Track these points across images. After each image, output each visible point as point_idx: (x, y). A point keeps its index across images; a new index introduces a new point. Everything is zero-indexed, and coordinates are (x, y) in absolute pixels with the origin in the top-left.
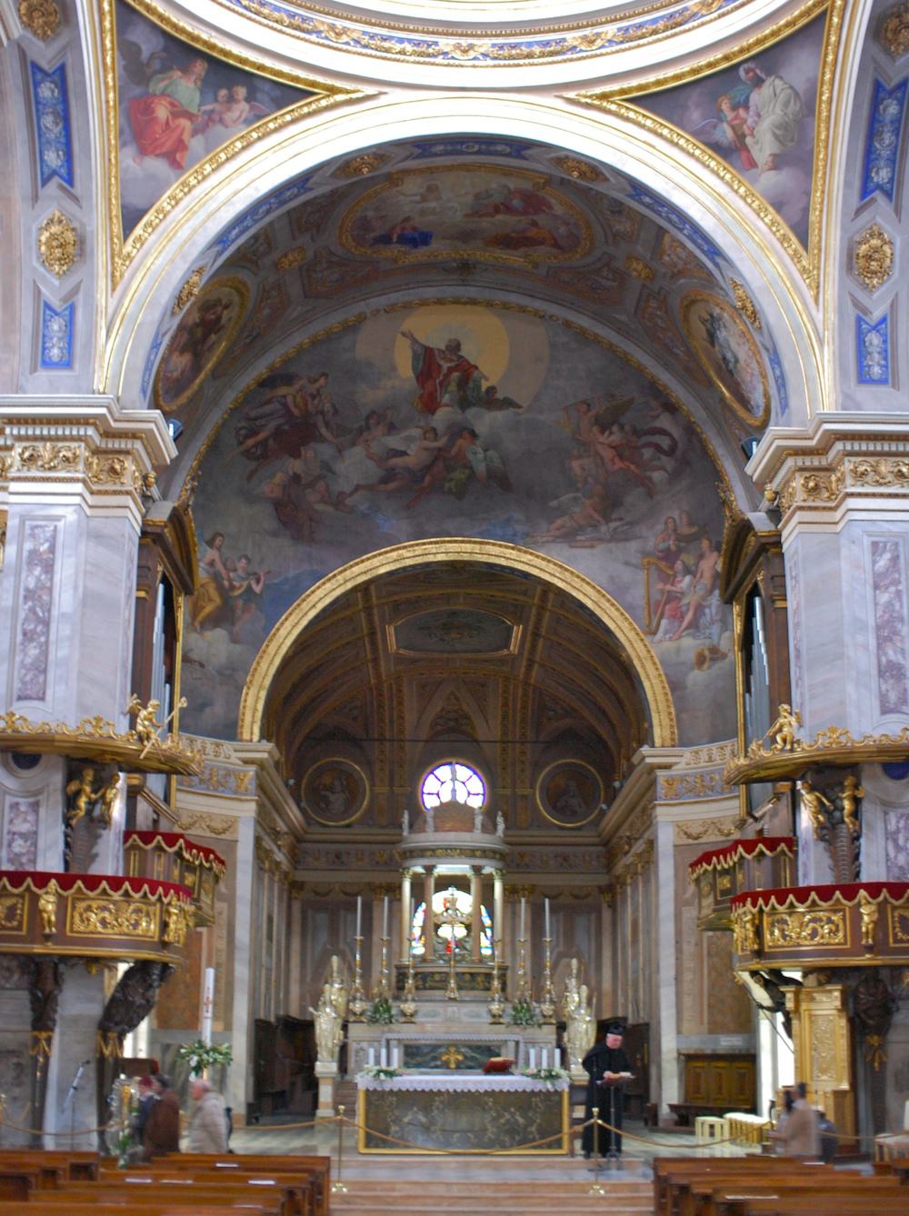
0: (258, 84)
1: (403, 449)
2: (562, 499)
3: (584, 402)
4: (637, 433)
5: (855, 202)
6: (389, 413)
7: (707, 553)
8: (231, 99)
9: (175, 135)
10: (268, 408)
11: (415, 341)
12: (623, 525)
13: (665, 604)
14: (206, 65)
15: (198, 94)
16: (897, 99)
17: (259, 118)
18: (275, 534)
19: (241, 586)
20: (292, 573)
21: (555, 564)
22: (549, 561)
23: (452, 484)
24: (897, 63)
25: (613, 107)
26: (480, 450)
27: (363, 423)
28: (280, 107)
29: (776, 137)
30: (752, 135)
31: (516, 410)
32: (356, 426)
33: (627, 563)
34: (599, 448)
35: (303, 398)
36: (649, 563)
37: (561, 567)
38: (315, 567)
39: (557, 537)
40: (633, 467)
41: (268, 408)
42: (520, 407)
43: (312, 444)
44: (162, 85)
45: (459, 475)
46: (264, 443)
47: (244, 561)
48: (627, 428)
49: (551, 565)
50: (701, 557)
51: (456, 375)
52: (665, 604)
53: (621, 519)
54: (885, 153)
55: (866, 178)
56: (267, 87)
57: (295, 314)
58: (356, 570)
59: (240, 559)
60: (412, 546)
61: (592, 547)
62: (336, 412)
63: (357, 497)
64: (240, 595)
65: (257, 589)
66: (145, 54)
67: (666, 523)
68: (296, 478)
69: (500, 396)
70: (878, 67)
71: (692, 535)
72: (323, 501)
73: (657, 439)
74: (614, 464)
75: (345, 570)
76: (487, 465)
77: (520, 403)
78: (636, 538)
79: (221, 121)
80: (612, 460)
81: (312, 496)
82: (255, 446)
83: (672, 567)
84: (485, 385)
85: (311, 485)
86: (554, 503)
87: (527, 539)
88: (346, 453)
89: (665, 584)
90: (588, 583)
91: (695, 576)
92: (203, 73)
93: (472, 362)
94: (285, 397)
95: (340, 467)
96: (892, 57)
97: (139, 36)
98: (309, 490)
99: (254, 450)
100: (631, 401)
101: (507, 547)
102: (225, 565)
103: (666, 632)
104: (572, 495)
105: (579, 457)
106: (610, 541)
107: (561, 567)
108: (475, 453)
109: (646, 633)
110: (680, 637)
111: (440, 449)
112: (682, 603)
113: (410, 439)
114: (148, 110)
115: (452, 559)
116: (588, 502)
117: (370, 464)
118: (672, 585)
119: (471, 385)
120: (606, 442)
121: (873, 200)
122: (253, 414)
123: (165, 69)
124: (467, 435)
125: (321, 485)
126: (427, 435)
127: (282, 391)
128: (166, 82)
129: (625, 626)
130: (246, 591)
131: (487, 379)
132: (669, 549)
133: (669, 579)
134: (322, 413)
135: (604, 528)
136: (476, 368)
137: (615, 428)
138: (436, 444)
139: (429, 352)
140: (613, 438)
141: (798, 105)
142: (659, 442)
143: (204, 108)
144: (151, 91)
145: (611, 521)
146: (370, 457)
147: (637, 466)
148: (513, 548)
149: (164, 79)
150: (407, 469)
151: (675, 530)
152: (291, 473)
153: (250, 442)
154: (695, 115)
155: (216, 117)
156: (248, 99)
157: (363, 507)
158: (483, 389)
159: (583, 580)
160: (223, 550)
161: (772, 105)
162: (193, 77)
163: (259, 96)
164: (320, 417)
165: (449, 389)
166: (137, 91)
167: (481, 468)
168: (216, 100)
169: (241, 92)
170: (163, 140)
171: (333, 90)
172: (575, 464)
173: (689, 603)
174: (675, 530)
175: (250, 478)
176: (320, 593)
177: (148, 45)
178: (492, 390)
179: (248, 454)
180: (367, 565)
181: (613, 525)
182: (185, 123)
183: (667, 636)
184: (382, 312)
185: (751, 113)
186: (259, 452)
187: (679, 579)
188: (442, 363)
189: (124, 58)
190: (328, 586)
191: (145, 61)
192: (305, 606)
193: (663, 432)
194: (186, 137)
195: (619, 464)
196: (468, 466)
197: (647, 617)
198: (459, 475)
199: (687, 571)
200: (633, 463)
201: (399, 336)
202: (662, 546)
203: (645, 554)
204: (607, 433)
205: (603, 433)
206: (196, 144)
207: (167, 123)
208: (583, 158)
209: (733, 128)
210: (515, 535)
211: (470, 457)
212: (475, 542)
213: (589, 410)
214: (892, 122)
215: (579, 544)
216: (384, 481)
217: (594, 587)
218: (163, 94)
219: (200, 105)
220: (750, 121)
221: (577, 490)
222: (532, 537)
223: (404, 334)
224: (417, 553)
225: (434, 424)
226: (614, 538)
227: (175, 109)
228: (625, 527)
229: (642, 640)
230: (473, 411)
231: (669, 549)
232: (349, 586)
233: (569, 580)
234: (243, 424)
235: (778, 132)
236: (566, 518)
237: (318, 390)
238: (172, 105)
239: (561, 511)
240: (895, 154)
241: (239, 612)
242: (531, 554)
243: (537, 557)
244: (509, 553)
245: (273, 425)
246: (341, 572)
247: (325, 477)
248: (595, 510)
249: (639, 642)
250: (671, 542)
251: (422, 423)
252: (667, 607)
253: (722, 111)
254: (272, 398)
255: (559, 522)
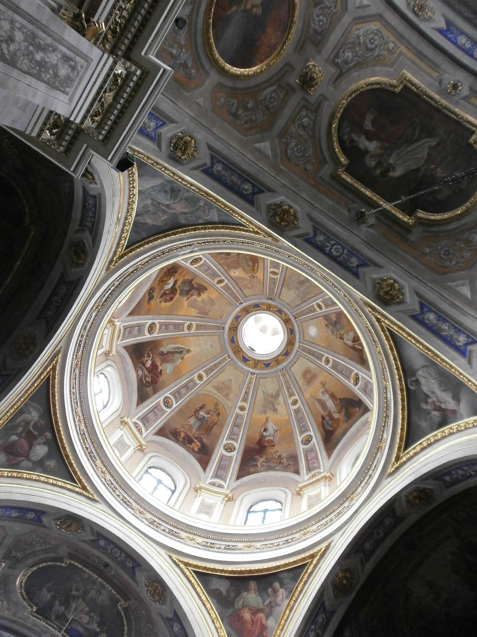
0: (281, 576)
5: (463, 361)
8: (275, 591)
9: (259, 624)
14: (255, 582)
15: (259, 598)
16: (428, 312)
17: (290, 592)
24: (409, 302)
25: (404, 459)
28: (296, 581)
29: (444, 391)
30: (441, 402)
44: (240, 603)
54: (452, 332)
55: (457, 349)
56: (285, 575)
66: (224, 592)
70: (404, 312)
79: (277, 604)
92: (256, 587)
96: (402, 302)
97: (216, 584)
114: (240, 618)
121: (470, 351)
123: (238, 594)
128: (242, 600)
141: (431, 368)
143: (266, 603)
144: (237, 608)
149: (240, 600)
154: (423, 424)
155: (273, 604)
156: (282, 587)
161: (430, 383)
162: (253, 591)
163: (285, 581)
166: (230, 611)
168: (269, 596)
169: (277, 585)
170: (254, 629)
171: (313, 556)
177: (223, 587)
182: (261, 615)
185: (431, 396)
189: (215, 599)
191: (227, 595)
194: (264, 621)
206: (271, 623)
207: (252, 620)
208: (409, 489)
209: (435, 410)
214: (438, 320)
218: (243, 607)
219: (263, 602)
220: (435, 399)
227: (253, 611)
235: (442, 388)
238: (250, 610)
240: (456, 327)
253: (426, 409)
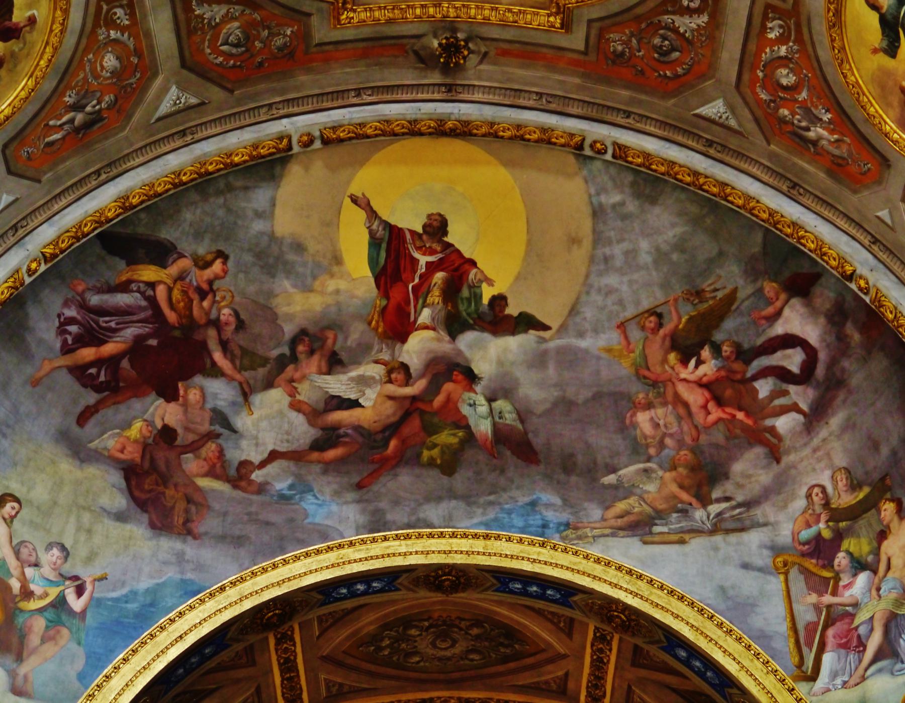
1: (353, 396)
2: (621, 472)
3: (652, 312)
4: (745, 355)
6: (330, 335)
7: (895, 525)
10: (122, 299)
11: (372, 214)
12: (734, 508)
13: (826, 627)
18: (120, 517)
19: (46, 595)
20: (144, 584)
21: (619, 568)
22: (608, 564)
23: (435, 452)
26: (481, 400)
27: (286, 350)
31: (542, 333)
32: (275, 353)
33: (746, 566)
34: (682, 389)
35: (185, 293)
36: (785, 564)
37: (630, 572)
38: (189, 576)
39: (621, 529)
40: (740, 415)
41: (122, 299)
42: (546, 328)
43: (198, 379)
45: (447, 438)
46: (112, 362)
47: (56, 552)
48: (726, 349)
49: (612, 571)
50: (883, 535)
51: (439, 276)
52: (826, 627)
53: (727, 499)
57: (165, 107)
58: (262, 580)
59: (49, 547)
60: (363, 542)
61: (682, 542)
62: (241, 325)
63: (272, 469)
64: (41, 610)
65: (76, 604)
67: (809, 496)
68: (167, 434)
69: (512, 310)
71: (860, 502)
72: (211, 473)
73: (777, 359)
74: (708, 413)
75: (242, 580)
76: (495, 425)
77: (547, 322)
78: (757, 525)
80: (705, 407)
81: (191, 464)
82: (98, 362)
83: (829, 565)
84: (487, 293)
85: (193, 448)
86: (610, 479)
87: (569, 532)
88: (257, 399)
89: (821, 594)
90: (681, 598)
91: (875, 572)
93: (467, 255)
94: (152, 285)
95: (243, 421)
98: (190, 455)
99: (93, 371)
100: (732, 297)
101: (532, 543)
102: (17, 554)
103: (834, 675)
104: (641, 466)
105: (649, 406)
106: (713, 531)
107: (630, 572)
108: (473, 405)
109: (796, 679)
110: (863, 679)
111: (414, 399)
112: (857, 622)
113: (364, 381)
115: (435, 561)
116: (668, 475)
117: (298, 420)
118: (834, 593)
119: (465, 293)
120: (692, 377)
122: (95, 300)
124: (460, 377)
125: (211, 448)
126: (393, 376)
127: (149, 273)
129: (756, 667)
130: (52, 605)
131: (490, 283)
132: (819, 535)
133: (832, 585)
134: (216, 324)
135: (699, 514)
136: (473, 263)
137: (706, 353)
138: (408, 391)
139: (395, 233)
140: (703, 369)
142: (785, 364)
145: (711, 502)
146: (296, 406)
147: (748, 415)
148: (543, 545)
150: (358, 428)
151: (827, 504)
152: (159, 425)
153: (88, 354)
157: (281, 485)
158: (485, 300)
159: (671, 592)
160: (16, 523)
164: (212, 333)
165: (430, 300)
167: (483, 427)
172: (643, 419)
173: (872, 618)
174: (827, 504)
175: (83, 418)
176: (192, 618)
178: (499, 301)
179: (79, 372)
180: (283, 572)
181: (714, 509)
183: (839, 681)
184: (318, 144)
186: (102, 378)
187: (845, 580)
188: (416, 255)
190: (211, 606)
192: (163, 639)
193: (790, 341)
195: (716, 413)
196: (462, 423)
197: (795, 653)
198: (447, 438)
199: (859, 565)
200: (740, 409)
201: (347, 201)
202: (806, 534)
203: (776, 550)
204: (693, 362)
205: (685, 362)
210: (545, 526)
211: (465, 410)
212: (476, 536)
213: (660, 325)
215: (657, 539)
216: (318, 446)
217: (692, 604)
221: (649, 459)
222: (576, 528)
223: (354, 200)
224: (372, 553)
225: (405, 358)
226: (718, 527)
228: (738, 511)
229: (791, 690)
230: (467, 339)
231: (819, 535)
232: (247, 605)
233: (646, 594)
234: (71, 312)
236: (632, 500)
237: (210, 282)
239: (621, 491)
241: (34, 640)
242: (576, 553)
243: (587, 557)
244: (535, 552)
245: (130, 332)
246: (233, 584)
247: (218, 436)
248: (681, 487)
249: (787, 694)
250: (822, 525)
251: (385, 356)
252: (830, 632)
254: (130, 282)
255: (621, 506)
